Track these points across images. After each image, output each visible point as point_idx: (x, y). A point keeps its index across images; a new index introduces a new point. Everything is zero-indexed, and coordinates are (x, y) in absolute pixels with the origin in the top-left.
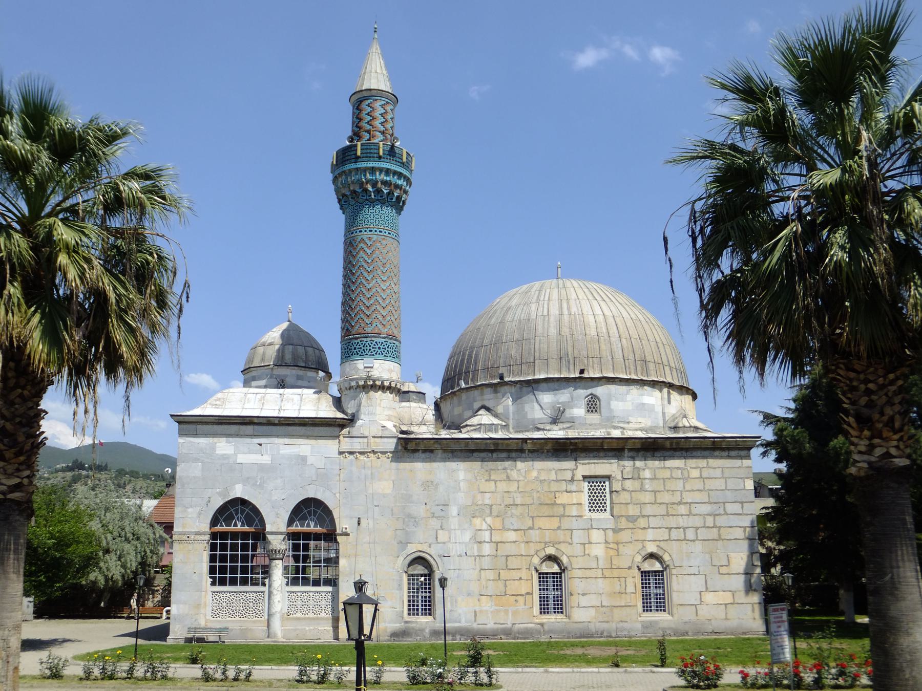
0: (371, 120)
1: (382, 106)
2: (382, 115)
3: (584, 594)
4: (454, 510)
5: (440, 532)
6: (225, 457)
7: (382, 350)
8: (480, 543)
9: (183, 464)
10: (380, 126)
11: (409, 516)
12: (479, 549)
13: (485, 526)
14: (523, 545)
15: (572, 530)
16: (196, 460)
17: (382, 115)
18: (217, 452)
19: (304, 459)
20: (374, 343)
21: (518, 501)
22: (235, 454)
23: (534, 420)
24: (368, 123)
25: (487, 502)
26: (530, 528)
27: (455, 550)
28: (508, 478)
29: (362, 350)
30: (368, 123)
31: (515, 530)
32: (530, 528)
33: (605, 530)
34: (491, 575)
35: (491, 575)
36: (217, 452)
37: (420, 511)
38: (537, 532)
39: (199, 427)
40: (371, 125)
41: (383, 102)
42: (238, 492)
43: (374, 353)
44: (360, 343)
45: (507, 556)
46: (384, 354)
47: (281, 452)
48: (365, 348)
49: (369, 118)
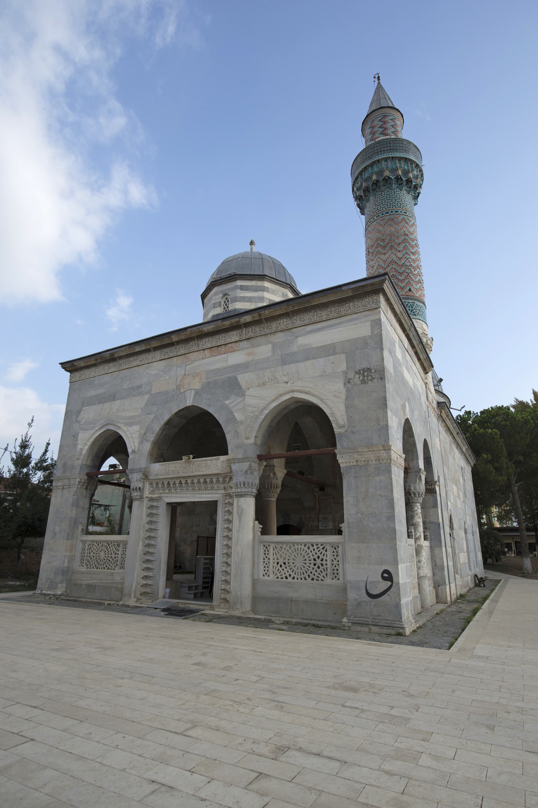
1: (392, 119)
2: (392, 126)
41: (392, 117)
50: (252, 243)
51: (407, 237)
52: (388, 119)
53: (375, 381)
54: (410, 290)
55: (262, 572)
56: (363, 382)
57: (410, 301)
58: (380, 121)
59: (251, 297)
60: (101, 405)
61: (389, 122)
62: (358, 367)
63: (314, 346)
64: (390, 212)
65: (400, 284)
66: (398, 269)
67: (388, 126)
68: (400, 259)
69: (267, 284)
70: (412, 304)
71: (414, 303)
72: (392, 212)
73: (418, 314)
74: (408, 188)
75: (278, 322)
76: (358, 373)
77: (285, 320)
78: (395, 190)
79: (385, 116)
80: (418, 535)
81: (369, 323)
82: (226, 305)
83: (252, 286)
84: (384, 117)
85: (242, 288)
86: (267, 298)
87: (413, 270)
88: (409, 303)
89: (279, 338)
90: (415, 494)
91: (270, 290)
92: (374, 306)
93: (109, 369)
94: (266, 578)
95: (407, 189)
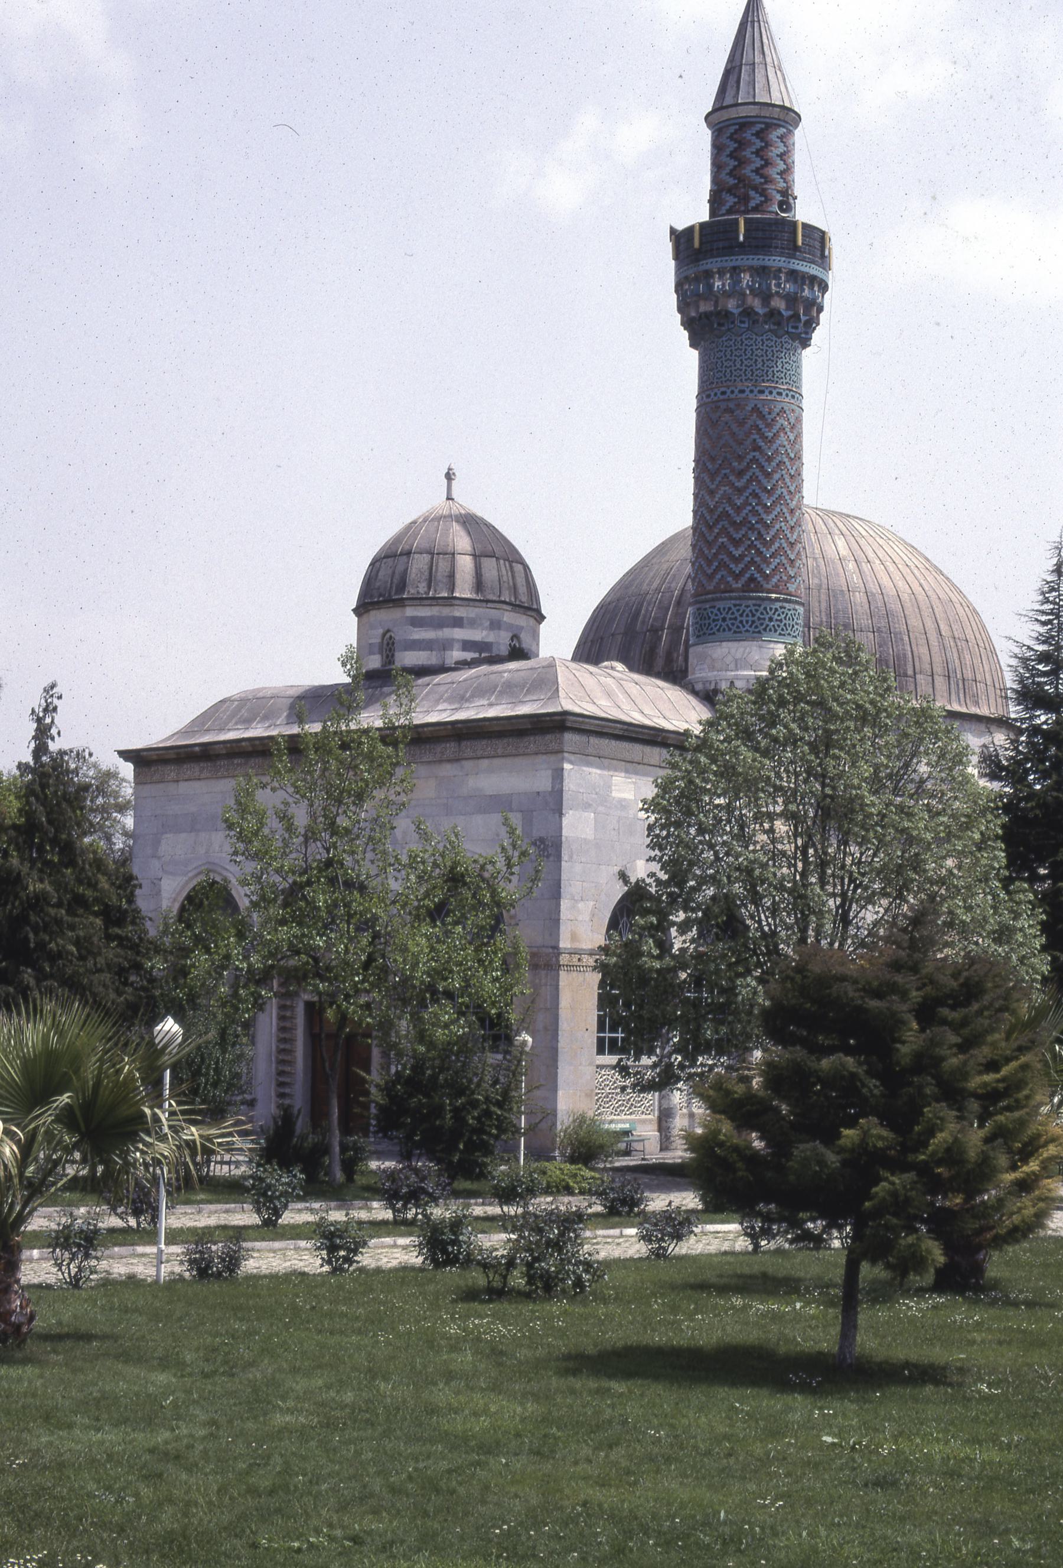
0: (762, 167)
2: (757, 153)
7: (729, 622)
9: (571, 812)
10: (753, 176)
16: (587, 806)
17: (757, 153)
18: (615, 794)
24: (757, 171)
36: (615, 794)
39: (594, 740)
40: (762, 176)
44: (734, 609)
48: (744, 619)
49: (759, 163)
50: (449, 476)
51: (757, 454)
52: (748, 135)
53: (551, 858)
57: (750, 602)
58: (731, 138)
60: (193, 834)
61: (750, 143)
62: (536, 834)
63: (488, 793)
64: (729, 391)
66: (731, 530)
67: (747, 153)
68: (738, 510)
70: (753, 608)
71: (760, 606)
72: (732, 392)
73: (765, 630)
74: (774, 324)
75: (443, 745)
76: (534, 844)
77: (453, 744)
78: (744, 337)
82: (390, 650)
84: (740, 129)
86: (458, 640)
87: (763, 531)
88: (747, 606)
89: (447, 770)
91: (465, 621)
93: (201, 771)
95: (772, 327)
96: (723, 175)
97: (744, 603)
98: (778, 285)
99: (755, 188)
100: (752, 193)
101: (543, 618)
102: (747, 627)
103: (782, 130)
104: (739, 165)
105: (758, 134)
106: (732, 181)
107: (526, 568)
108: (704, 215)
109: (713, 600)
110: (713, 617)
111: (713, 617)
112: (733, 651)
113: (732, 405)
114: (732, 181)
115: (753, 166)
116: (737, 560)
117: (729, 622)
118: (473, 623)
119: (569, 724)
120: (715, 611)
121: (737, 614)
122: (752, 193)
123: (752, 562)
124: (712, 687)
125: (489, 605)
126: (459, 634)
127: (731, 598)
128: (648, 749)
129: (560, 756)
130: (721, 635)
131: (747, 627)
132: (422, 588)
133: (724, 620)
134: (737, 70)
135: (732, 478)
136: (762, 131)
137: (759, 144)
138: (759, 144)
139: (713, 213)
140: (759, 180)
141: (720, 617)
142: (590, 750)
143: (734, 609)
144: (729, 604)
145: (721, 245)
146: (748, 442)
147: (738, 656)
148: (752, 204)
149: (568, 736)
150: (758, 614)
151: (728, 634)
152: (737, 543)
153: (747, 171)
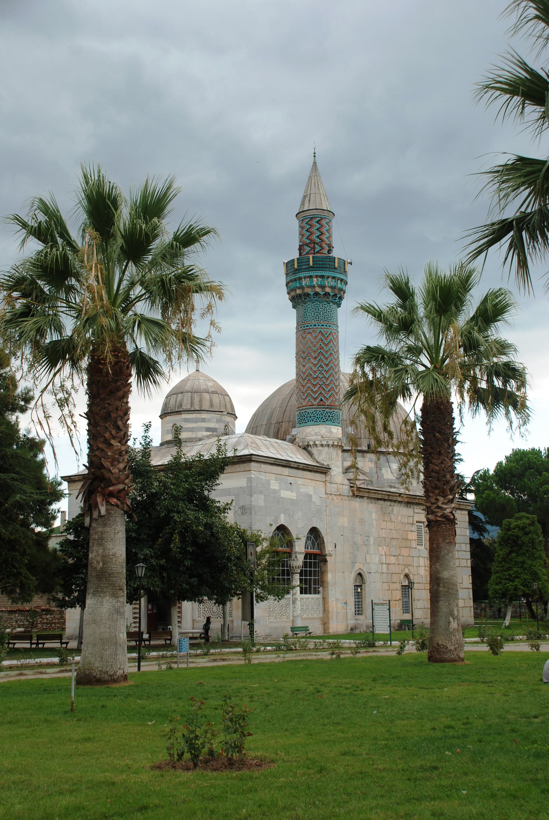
1: (318, 222)
2: (318, 229)
3: (419, 600)
4: (372, 540)
5: (367, 555)
6: (275, 492)
8: (382, 564)
10: (317, 239)
11: (355, 543)
12: (382, 568)
13: (383, 553)
14: (397, 566)
15: (413, 557)
16: (261, 492)
17: (318, 229)
18: (271, 487)
19: (310, 496)
20: (325, 412)
21: (395, 537)
22: (280, 490)
23: (388, 480)
24: (318, 237)
25: (384, 536)
26: (399, 555)
27: (373, 568)
28: (391, 520)
29: (316, 418)
30: (318, 237)
31: (394, 556)
32: (399, 555)
33: (424, 558)
34: (386, 586)
35: (386, 586)
36: (271, 487)
37: (359, 539)
38: (402, 557)
39: (263, 466)
41: (318, 219)
42: (282, 521)
43: (325, 420)
45: (392, 573)
46: (315, 420)
47: (301, 491)
51: (321, 350)
52: (314, 222)
53: (248, 514)
54: (321, 400)
55: (197, 616)
56: (243, 514)
59: (193, 428)
62: (241, 504)
65: (313, 395)
67: (314, 230)
69: (204, 416)
79: (312, 219)
80: (295, 592)
81: (246, 479)
83: (193, 418)
85: (186, 420)
87: (325, 381)
90: (293, 567)
92: (248, 469)
94: (199, 618)
96: (304, 239)
97: (318, 410)
98: (328, 283)
99: (317, 244)
100: (316, 246)
101: (237, 418)
102: (320, 419)
103: (327, 220)
104: (311, 234)
105: (318, 222)
106: (308, 241)
107: (230, 398)
108: (298, 257)
109: (306, 409)
110: (306, 416)
111: (306, 416)
112: (314, 429)
113: (311, 331)
114: (308, 241)
115: (316, 235)
116: (315, 393)
117: (312, 418)
118: (209, 420)
119: (253, 459)
120: (307, 413)
121: (316, 415)
122: (316, 246)
123: (321, 393)
124: (307, 444)
125: (216, 413)
126: (204, 425)
127: (313, 408)
128: (284, 469)
129: (250, 472)
130: (309, 423)
131: (320, 419)
132: (189, 407)
133: (310, 417)
134: (309, 196)
135: (312, 360)
136: (320, 220)
137: (318, 226)
138: (318, 226)
139: (300, 254)
140: (318, 241)
141: (309, 416)
142: (262, 470)
143: (314, 413)
144: (312, 410)
145: (305, 267)
146: (319, 345)
147: (316, 431)
148: (316, 250)
149: (253, 464)
150: (324, 414)
151: (312, 423)
152: (315, 386)
153: (314, 237)
